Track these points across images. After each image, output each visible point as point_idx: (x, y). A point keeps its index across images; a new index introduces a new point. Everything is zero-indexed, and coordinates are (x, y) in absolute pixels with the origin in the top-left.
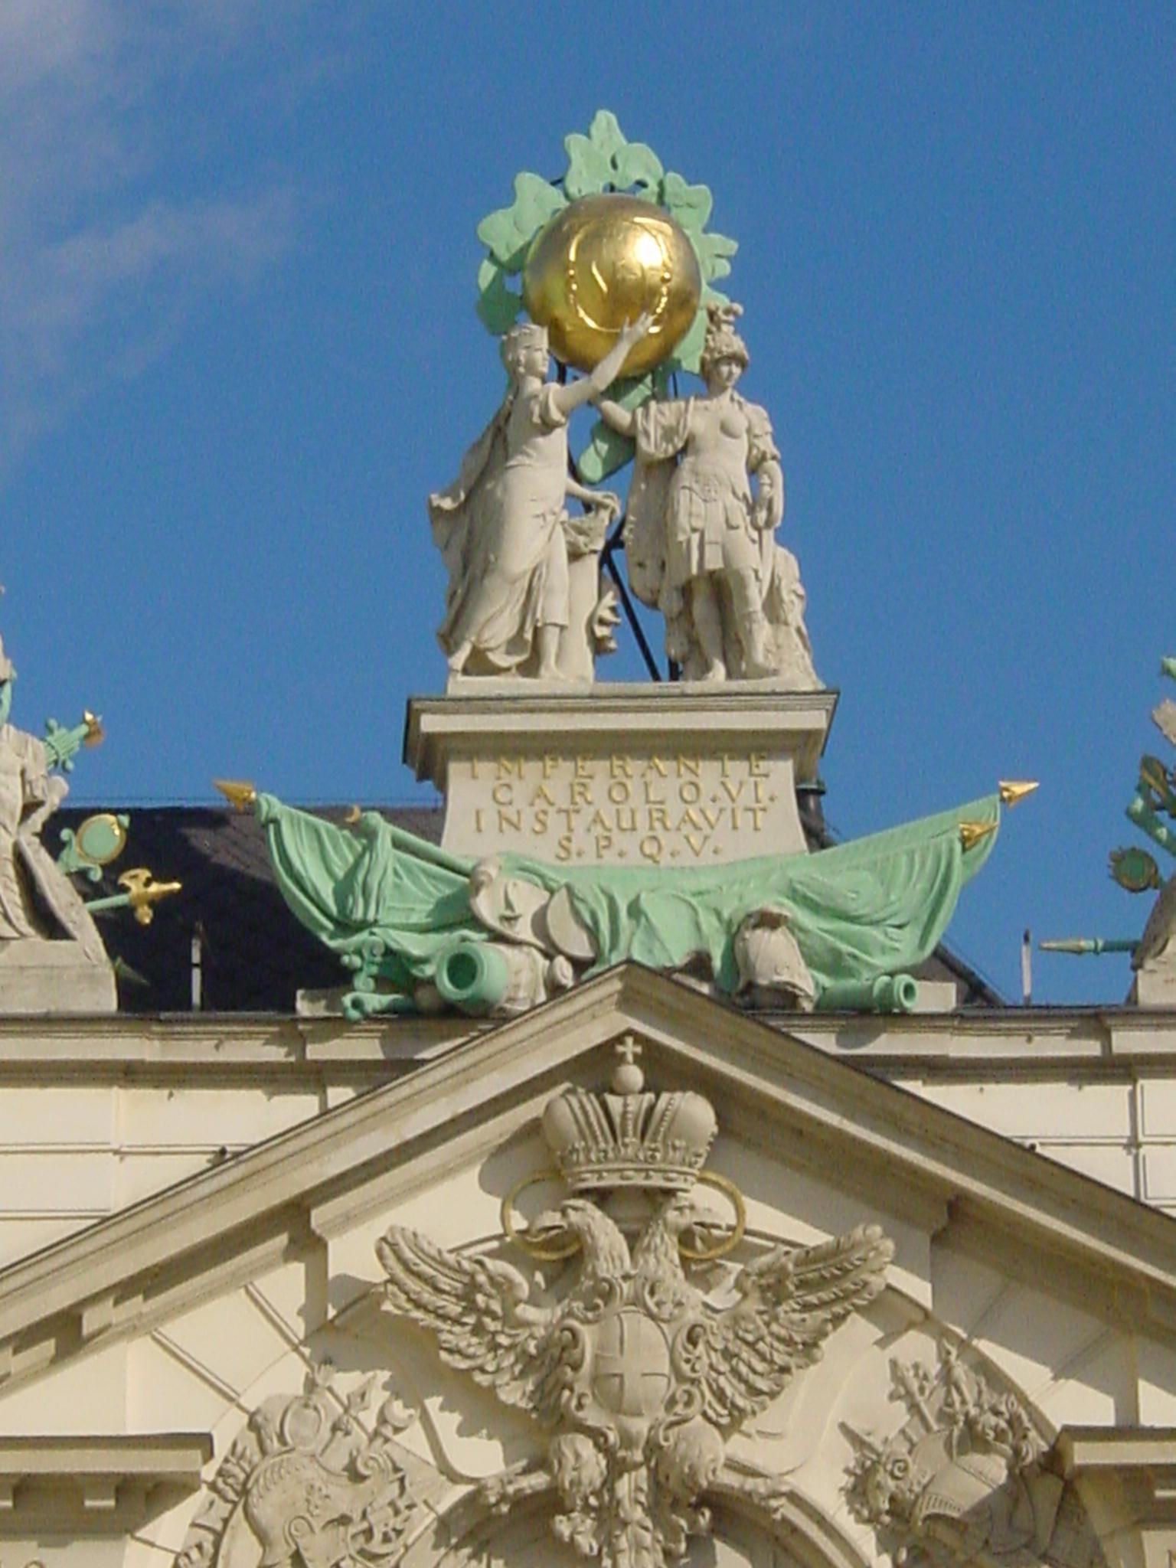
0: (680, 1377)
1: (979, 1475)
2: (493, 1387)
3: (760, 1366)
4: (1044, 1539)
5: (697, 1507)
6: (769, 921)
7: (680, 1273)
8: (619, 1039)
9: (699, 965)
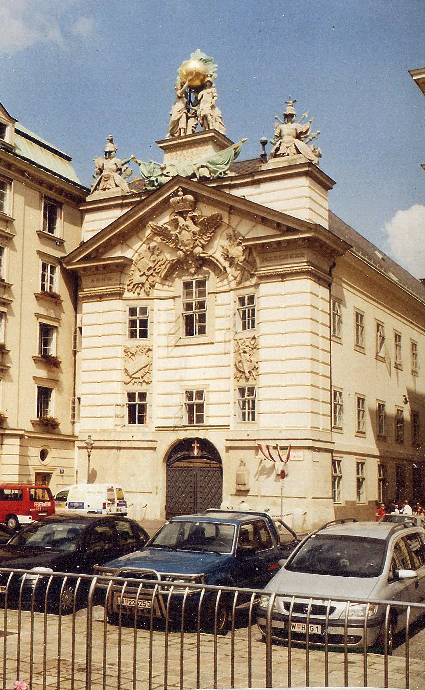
0: (192, 240)
1: (237, 250)
2: (169, 245)
3: (206, 237)
4: (247, 259)
5: (200, 260)
6: (202, 166)
7: (193, 224)
8: (179, 188)
9: (194, 176)
